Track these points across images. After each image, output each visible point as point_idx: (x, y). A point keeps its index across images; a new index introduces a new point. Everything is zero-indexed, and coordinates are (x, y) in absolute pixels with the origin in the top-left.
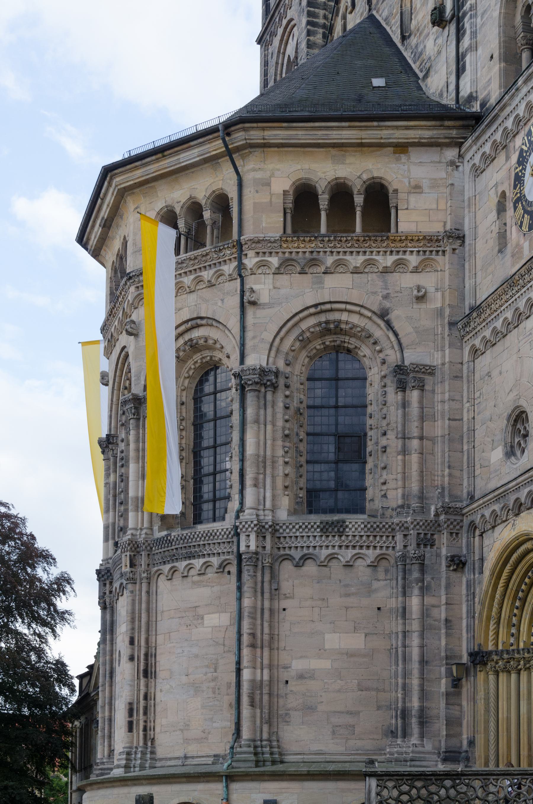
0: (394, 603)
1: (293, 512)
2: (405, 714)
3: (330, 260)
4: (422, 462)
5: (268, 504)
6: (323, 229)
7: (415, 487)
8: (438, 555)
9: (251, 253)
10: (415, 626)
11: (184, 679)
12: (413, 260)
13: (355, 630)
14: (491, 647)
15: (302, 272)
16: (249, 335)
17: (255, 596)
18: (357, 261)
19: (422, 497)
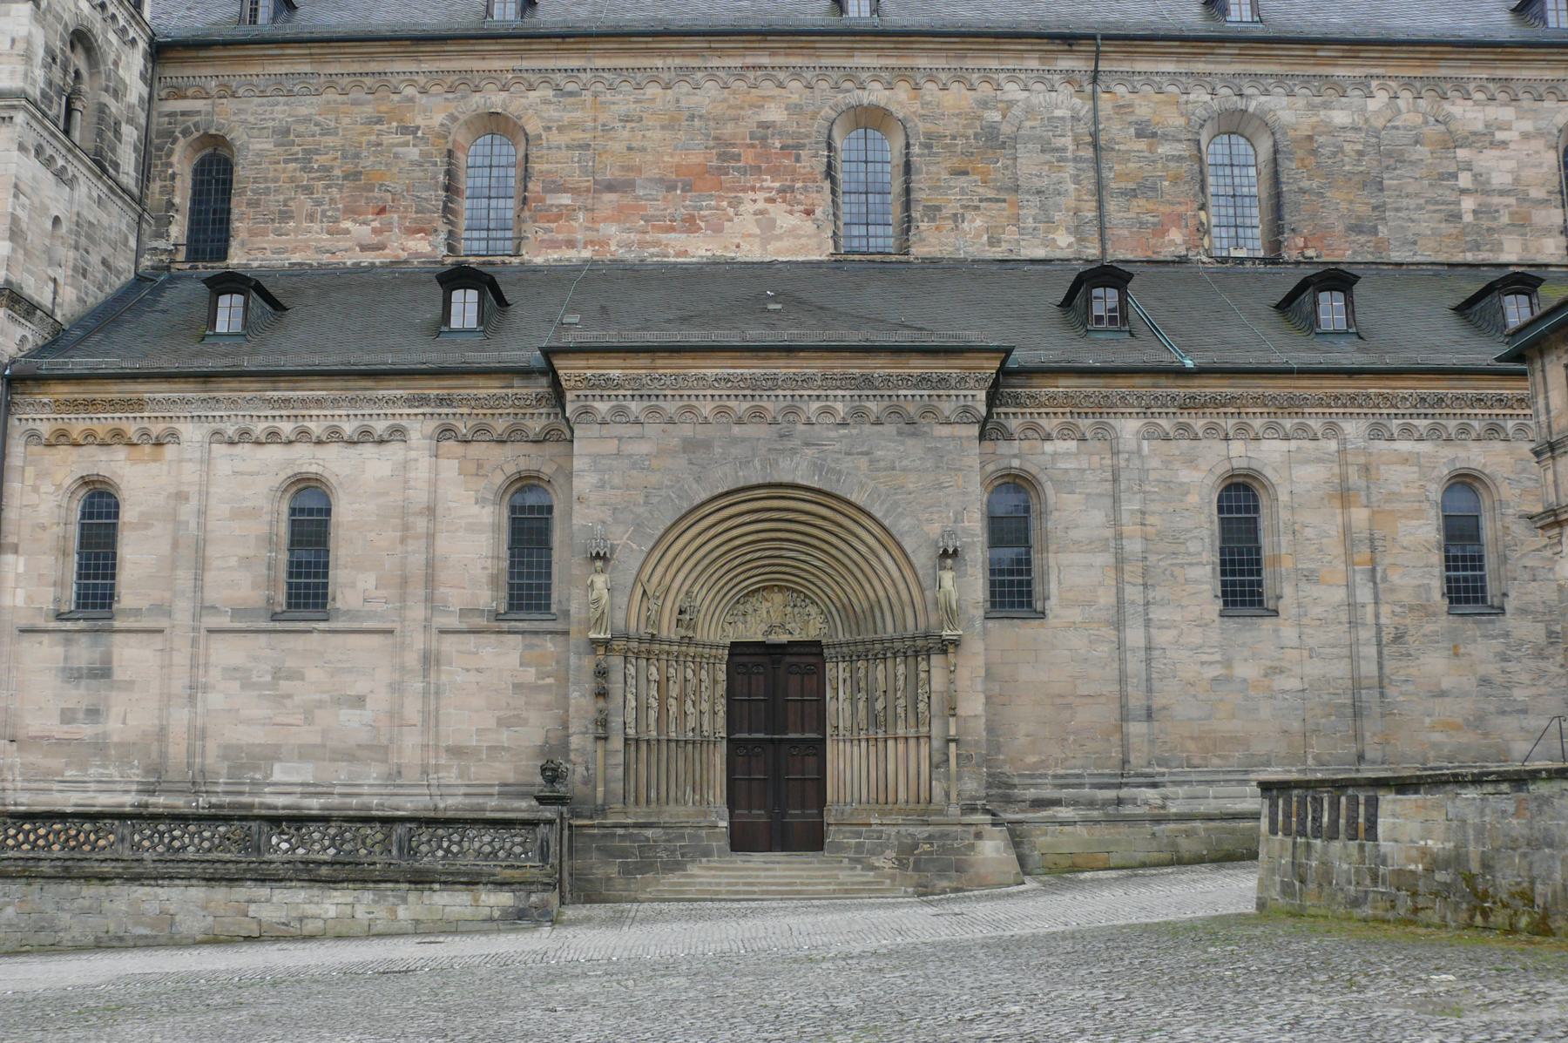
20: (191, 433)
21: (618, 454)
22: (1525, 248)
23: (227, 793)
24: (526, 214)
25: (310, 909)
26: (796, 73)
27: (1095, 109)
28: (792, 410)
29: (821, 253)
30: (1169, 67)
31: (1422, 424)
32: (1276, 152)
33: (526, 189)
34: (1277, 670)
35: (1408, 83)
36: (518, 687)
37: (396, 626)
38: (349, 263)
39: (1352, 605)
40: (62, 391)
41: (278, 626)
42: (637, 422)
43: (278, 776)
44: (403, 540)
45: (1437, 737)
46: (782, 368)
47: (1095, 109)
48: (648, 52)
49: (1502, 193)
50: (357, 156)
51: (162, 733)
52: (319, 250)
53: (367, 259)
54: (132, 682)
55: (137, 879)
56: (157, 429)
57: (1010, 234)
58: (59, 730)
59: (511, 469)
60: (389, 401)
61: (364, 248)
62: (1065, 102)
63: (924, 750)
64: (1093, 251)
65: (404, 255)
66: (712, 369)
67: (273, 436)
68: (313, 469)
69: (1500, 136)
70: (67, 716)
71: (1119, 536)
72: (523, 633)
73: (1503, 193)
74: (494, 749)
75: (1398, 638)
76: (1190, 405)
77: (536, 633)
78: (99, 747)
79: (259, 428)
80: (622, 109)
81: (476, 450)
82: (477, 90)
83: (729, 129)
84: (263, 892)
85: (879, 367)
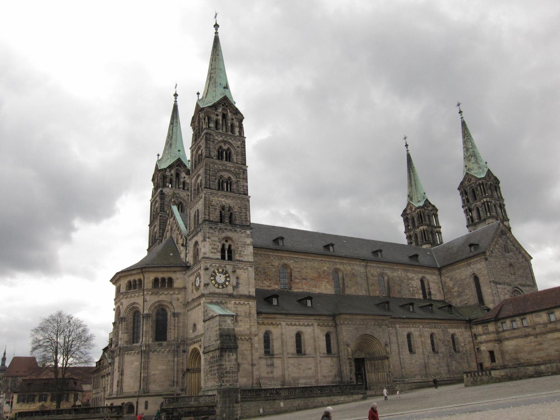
0: (172, 359)
1: (152, 341)
2: (173, 382)
3: (161, 293)
4: (178, 332)
5: (148, 340)
6: (160, 286)
7: (176, 336)
8: (181, 349)
9: (146, 291)
10: (176, 364)
11: (129, 376)
12: (177, 292)
13: (164, 365)
14: (190, 368)
15: (155, 295)
16: (145, 307)
17: (144, 359)
18: (166, 293)
19: (178, 338)
20: (283, 324)
21: (348, 330)
22: (418, 296)
23: (294, 385)
24: (292, 283)
25: (340, 399)
26: (328, 261)
27: (366, 271)
28: (367, 324)
29: (334, 293)
30: (375, 265)
31: (428, 326)
32: (388, 279)
33: (291, 278)
34: (416, 361)
35: (403, 270)
36: (331, 366)
37: (315, 356)
38: (266, 289)
39: (423, 352)
40: (264, 315)
41: (299, 356)
42: (350, 325)
43: (300, 382)
44: (314, 342)
45: (434, 371)
46: (367, 317)
47: (366, 271)
48: (308, 256)
49: (415, 288)
50: (265, 269)
51: (283, 375)
52: (260, 286)
53: (269, 288)
54: (277, 367)
55: (317, 397)
56: (278, 323)
57: (357, 291)
58: (267, 376)
59: (327, 331)
60: (312, 319)
61: (268, 287)
62: (362, 270)
63: (385, 373)
64: (368, 294)
65: (274, 288)
66: (359, 317)
67: (295, 325)
68: (301, 330)
69: (414, 279)
70: (268, 373)
71: (398, 342)
72: (331, 357)
73: (415, 288)
74: (329, 376)
75: (428, 357)
76: (404, 323)
77: (333, 357)
78: (273, 378)
79: (294, 323)
80: (305, 265)
81: (323, 328)
82: (283, 259)
83: (319, 270)
84: (334, 397)
85: (377, 318)
